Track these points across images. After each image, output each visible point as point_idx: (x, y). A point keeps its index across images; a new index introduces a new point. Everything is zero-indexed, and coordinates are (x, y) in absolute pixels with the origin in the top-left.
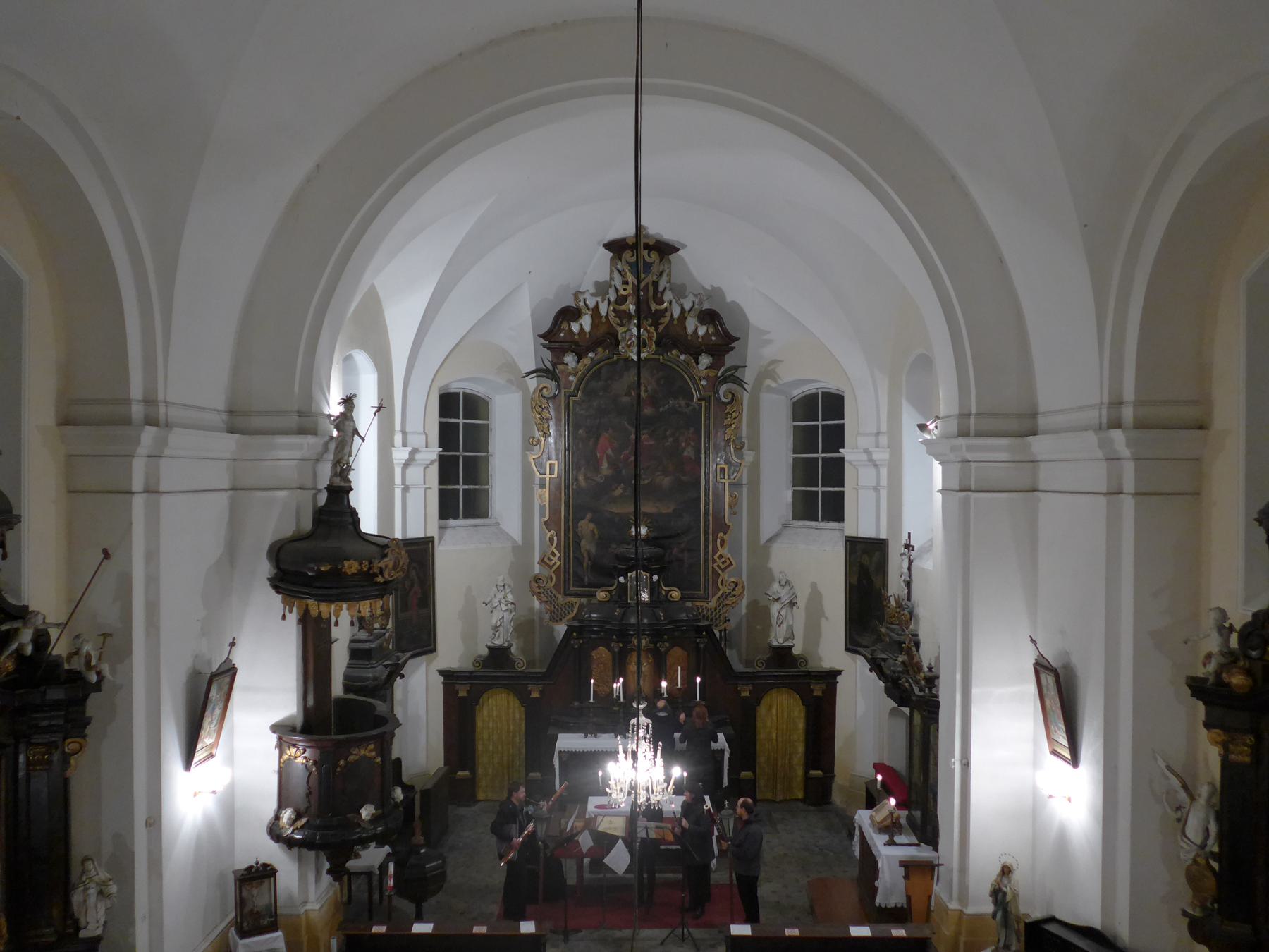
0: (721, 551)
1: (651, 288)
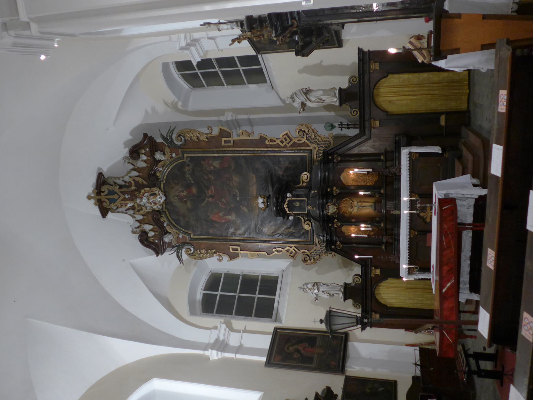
0: (278, 142)
1: (123, 190)
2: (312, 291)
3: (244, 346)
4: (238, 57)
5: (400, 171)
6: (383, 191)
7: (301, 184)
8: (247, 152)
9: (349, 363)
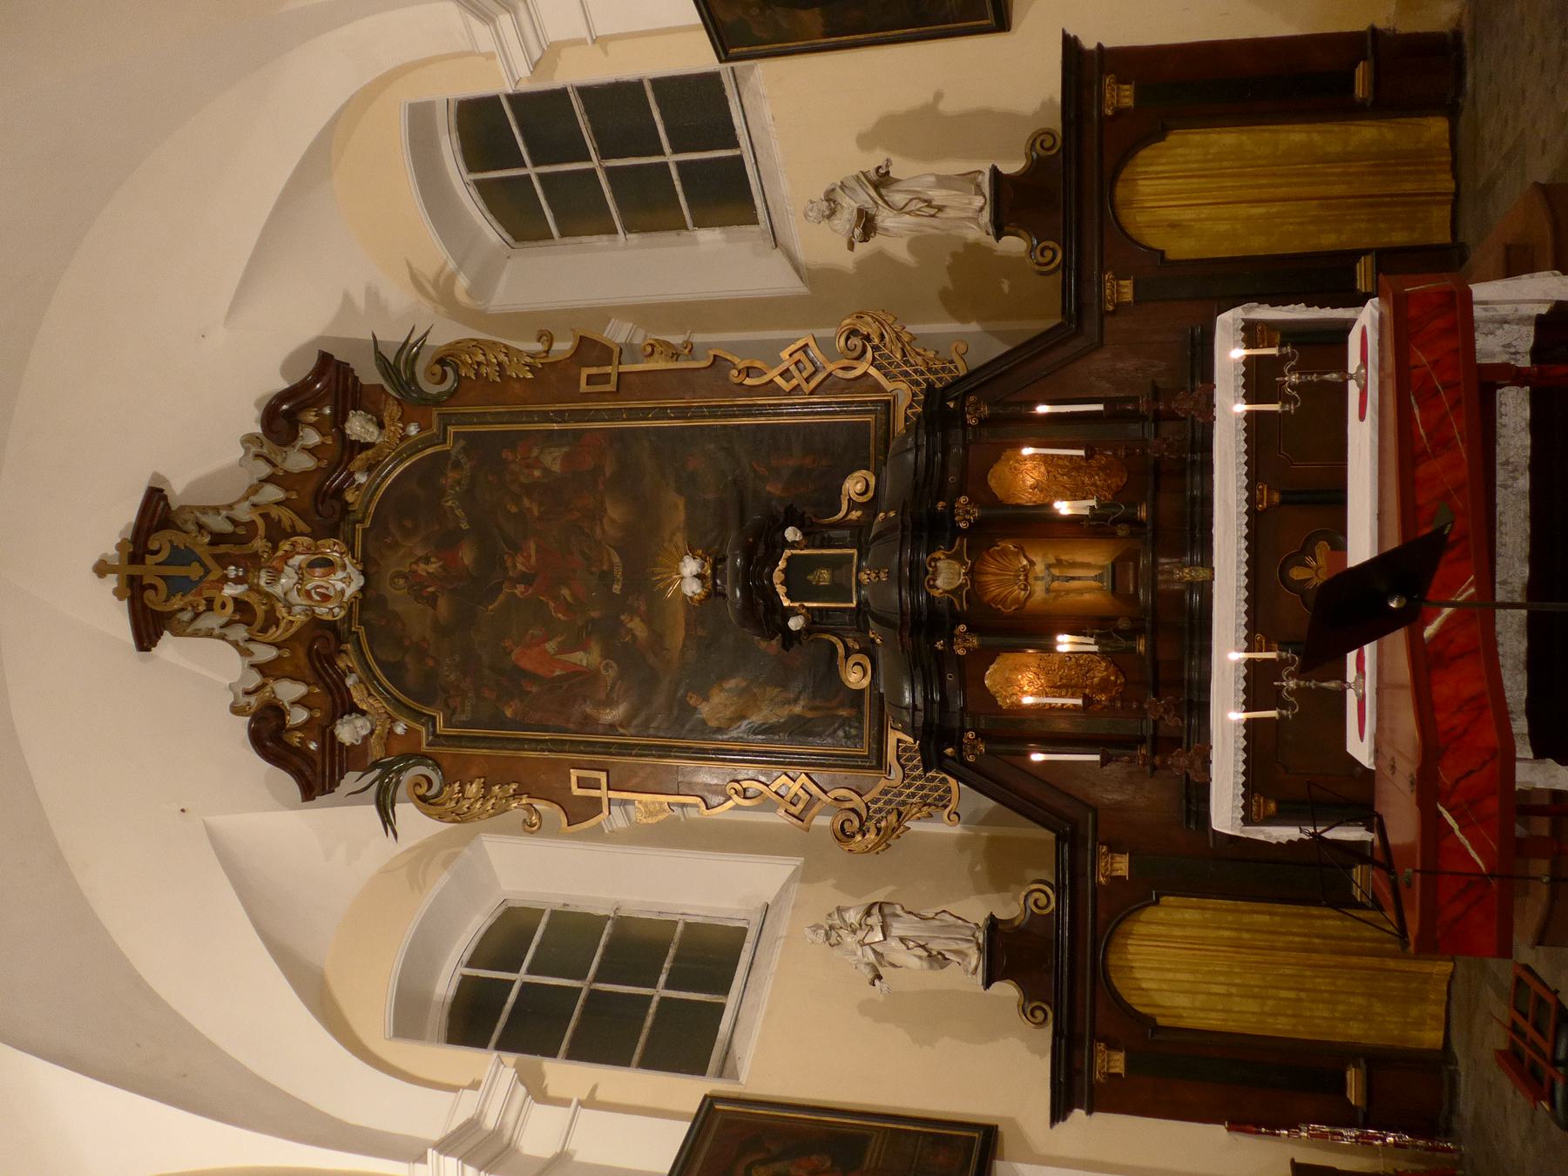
0: (773, 374)
1: (223, 549)
2: (860, 935)
3: (578, 1158)
4: (656, 83)
5: (1207, 770)
6: (1143, 513)
7: (841, 514)
8: (661, 413)
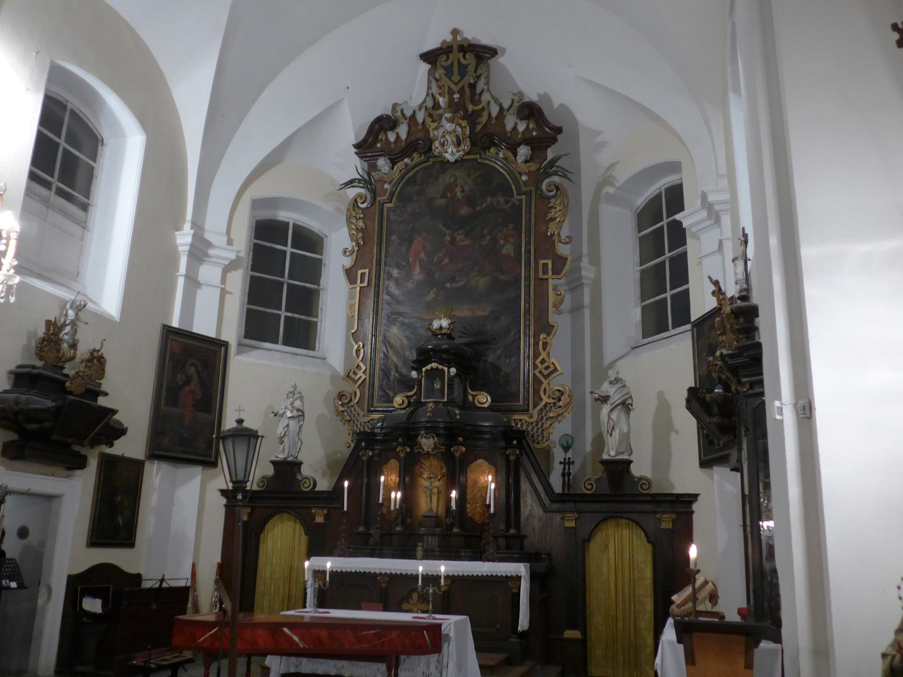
0: (543, 355)
1: (467, 90)
2: (290, 407)
4: (687, 290)
5: (489, 560)
6: (455, 530)
7: (470, 391)
8: (527, 302)
9: (165, 467)
